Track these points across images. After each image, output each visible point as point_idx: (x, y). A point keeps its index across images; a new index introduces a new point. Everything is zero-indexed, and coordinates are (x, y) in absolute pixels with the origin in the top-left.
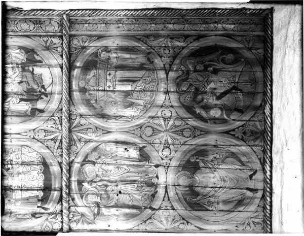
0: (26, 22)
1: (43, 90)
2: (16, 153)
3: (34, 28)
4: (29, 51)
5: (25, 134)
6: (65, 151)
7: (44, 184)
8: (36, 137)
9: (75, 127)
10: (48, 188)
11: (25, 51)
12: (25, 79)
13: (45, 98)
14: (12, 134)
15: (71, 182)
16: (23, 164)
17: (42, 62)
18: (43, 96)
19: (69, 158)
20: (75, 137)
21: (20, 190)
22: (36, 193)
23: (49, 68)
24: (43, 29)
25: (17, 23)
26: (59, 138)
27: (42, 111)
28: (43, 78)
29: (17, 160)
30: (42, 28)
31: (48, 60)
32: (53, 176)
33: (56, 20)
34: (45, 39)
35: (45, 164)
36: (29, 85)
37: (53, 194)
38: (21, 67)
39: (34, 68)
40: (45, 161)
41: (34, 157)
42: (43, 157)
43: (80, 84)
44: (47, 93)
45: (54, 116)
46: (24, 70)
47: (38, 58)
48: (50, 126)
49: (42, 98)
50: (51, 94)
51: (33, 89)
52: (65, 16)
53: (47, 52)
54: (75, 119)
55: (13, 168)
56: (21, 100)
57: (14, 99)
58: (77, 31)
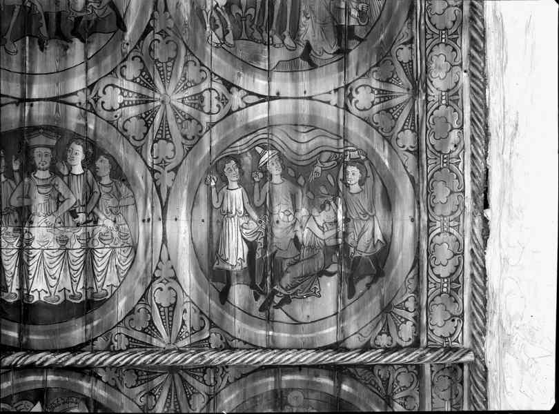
0: (455, 254)
1: (277, 300)
2: (116, 234)
3: (438, 276)
4: (381, 259)
5: (164, 257)
6: (122, 359)
7: (38, 304)
8: (157, 285)
9: (184, 381)
10: (27, 312)
11: (379, 253)
12: (305, 253)
13: (259, 304)
14: (164, 224)
15: (42, 373)
16: (89, 252)
17: (350, 296)
18: (262, 300)
19: (104, 368)
20: (157, 381)
21: (21, 245)
22: (14, 287)
23: (336, 314)
24: (438, 300)
25: (450, 234)
26: (155, 342)
27: (224, 296)
28: (309, 299)
29: (97, 237)
30: (440, 295)
31: (357, 310)
32: (57, 326)
33: (459, 329)
34: (410, 305)
35: (89, 306)
36: (290, 265)
37: (10, 329)
38: (338, 245)
39: (336, 275)
40: (99, 307)
41: (107, 279)
42: (106, 300)
43: (295, 393)
44: (271, 309)
45: (210, 328)
46: (330, 251)
47: (360, 287)
48: (186, 317)
49: (257, 298)
50: (270, 321)
51: (282, 274)
52: (469, 357)
53: (377, 310)
54: (204, 382)
55: (78, 225)
56: (252, 246)
57: (253, 226)
58: (433, 384)
